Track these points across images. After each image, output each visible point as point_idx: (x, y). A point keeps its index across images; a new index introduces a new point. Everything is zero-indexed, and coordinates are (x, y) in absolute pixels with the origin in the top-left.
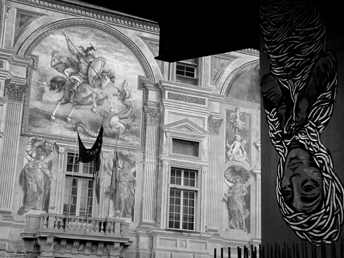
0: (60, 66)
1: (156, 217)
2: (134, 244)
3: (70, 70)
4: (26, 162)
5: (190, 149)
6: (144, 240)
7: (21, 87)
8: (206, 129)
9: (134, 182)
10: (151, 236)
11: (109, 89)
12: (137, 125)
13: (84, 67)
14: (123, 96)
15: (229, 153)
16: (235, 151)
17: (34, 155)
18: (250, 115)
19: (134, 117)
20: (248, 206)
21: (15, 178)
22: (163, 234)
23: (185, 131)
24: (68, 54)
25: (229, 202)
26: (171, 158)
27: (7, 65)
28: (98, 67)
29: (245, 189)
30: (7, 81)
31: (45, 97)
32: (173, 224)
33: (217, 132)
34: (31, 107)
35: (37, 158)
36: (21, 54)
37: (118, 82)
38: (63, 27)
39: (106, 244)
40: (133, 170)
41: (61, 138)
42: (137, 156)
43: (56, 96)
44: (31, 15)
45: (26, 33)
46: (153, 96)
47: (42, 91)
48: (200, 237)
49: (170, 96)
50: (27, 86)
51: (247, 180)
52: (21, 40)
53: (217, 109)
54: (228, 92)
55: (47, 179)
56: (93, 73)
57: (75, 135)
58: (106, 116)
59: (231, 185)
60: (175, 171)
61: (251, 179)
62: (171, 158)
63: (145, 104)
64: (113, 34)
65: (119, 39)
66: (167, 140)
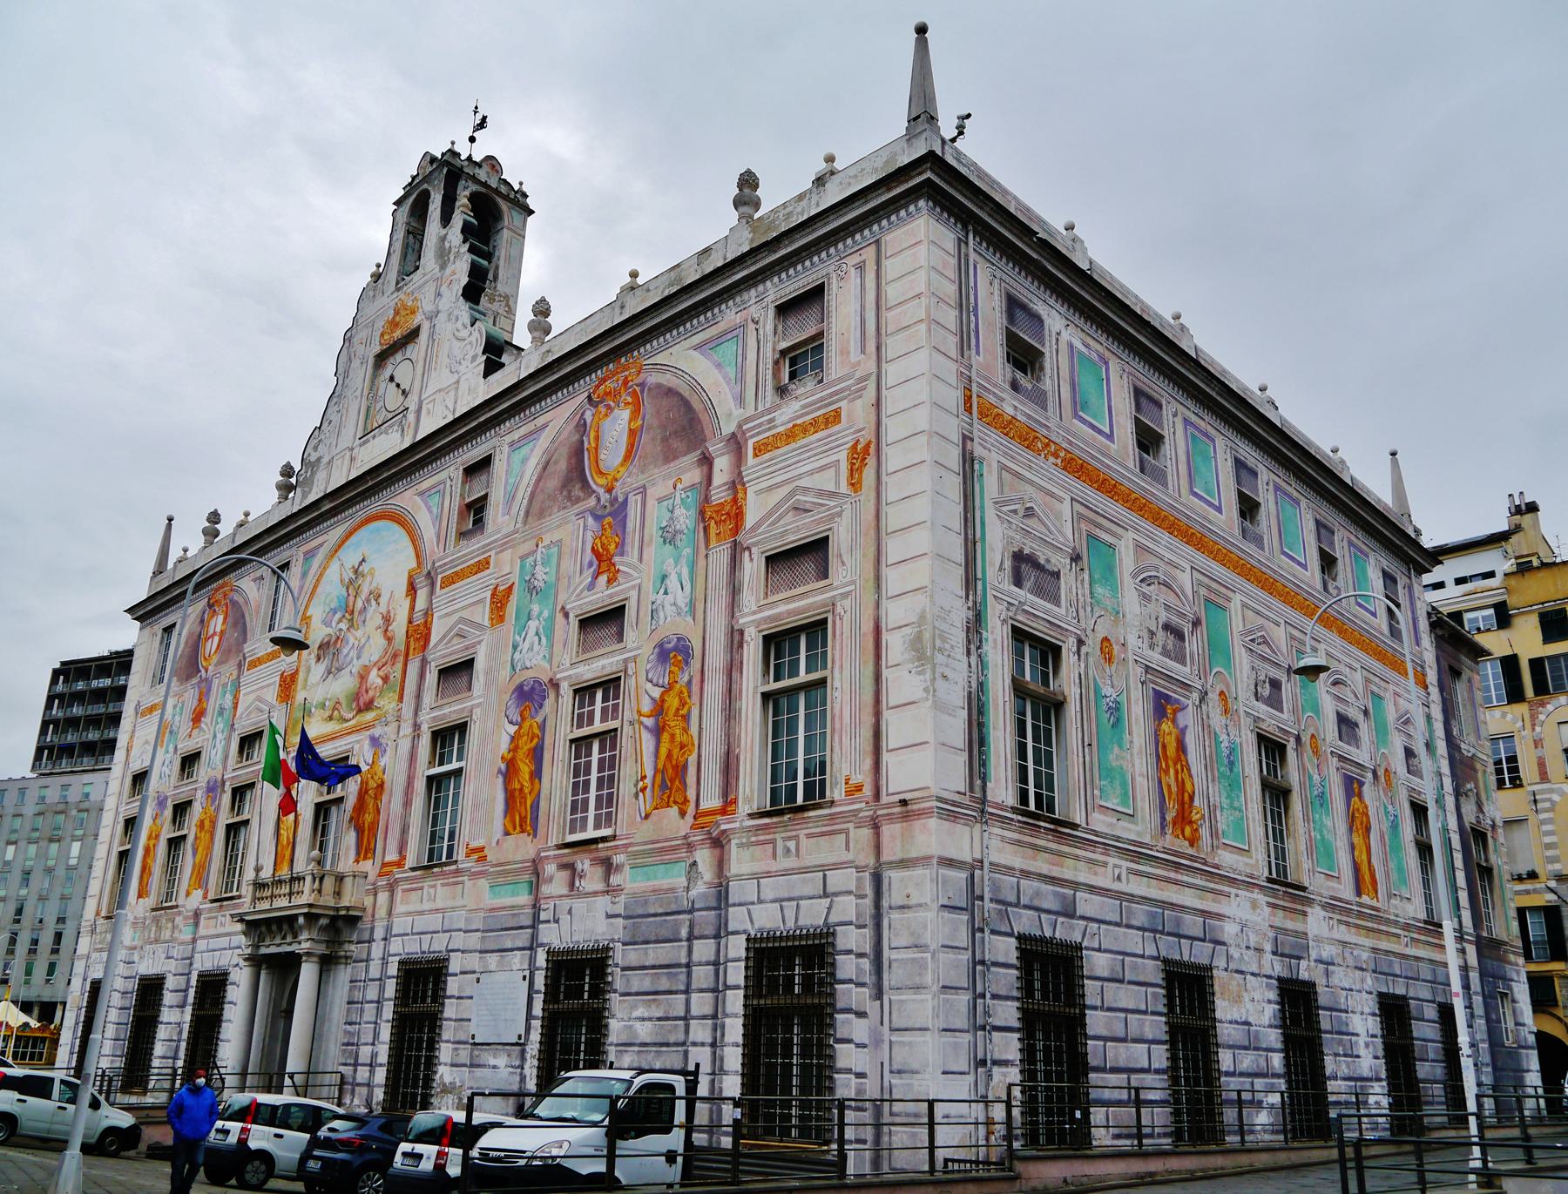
8: (487, 623)
15: (517, 656)
20: (537, 774)
22: (407, 879)
25: (510, 771)
28: (365, 591)
29: (536, 731)
47: (309, 671)
48: (458, 871)
50: (297, 671)
51: (541, 706)
54: (527, 513)
56: (359, 604)
59: (512, 729)
61: (549, 703)
63: (410, 622)
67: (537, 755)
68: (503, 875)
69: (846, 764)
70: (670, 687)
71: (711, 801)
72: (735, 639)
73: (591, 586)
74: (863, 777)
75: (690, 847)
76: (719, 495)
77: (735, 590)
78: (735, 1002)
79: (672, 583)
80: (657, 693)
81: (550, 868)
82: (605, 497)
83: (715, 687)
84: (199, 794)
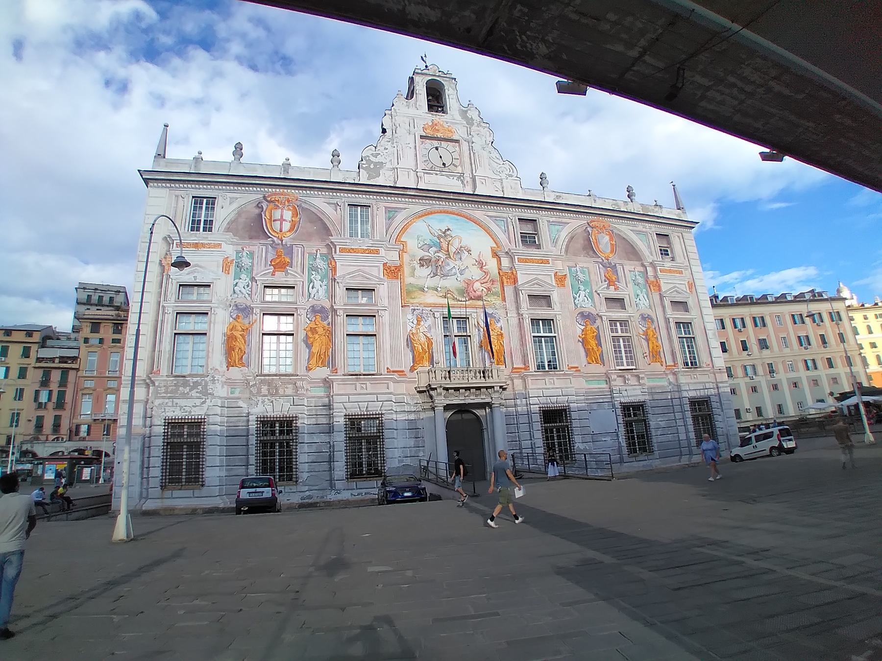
0: (427, 247)
1: (525, 361)
2: (510, 386)
3: (434, 249)
4: (409, 328)
5: (543, 302)
6: (518, 382)
7: (396, 267)
9: (502, 335)
10: (524, 379)
11: (468, 260)
12: (497, 288)
13: (445, 246)
14: (481, 265)
16: (581, 299)
17: (415, 322)
18: (588, 268)
19: (493, 281)
20: (599, 344)
21: (403, 343)
23: (536, 287)
24: (431, 237)
25: (584, 342)
26: (529, 311)
27: (382, 252)
30: (385, 264)
31: (417, 273)
32: (541, 367)
33: (563, 285)
34: (406, 283)
35: (418, 324)
36: (393, 241)
37: (475, 254)
38: (423, 216)
39: (487, 388)
40: (499, 325)
41: (435, 306)
42: (500, 313)
43: (426, 271)
44: (397, 210)
45: (394, 225)
46: (505, 262)
48: (565, 375)
49: (520, 260)
52: (391, 230)
53: (560, 266)
54: (567, 251)
55: (429, 341)
56: (452, 249)
57: (445, 301)
58: (469, 283)
60: (535, 321)
61: (598, 321)
62: (529, 311)
64: (463, 216)
65: (470, 219)
66: (524, 298)
67: (598, 338)
68: (589, 378)
69: (704, 358)
70: (648, 328)
71: (670, 362)
72: (667, 321)
73: (608, 288)
74: (709, 362)
75: (666, 374)
76: (652, 279)
77: (664, 307)
78: (689, 414)
79: (641, 297)
80: (644, 329)
81: (614, 377)
82: (605, 261)
83: (664, 332)
84: (303, 312)
